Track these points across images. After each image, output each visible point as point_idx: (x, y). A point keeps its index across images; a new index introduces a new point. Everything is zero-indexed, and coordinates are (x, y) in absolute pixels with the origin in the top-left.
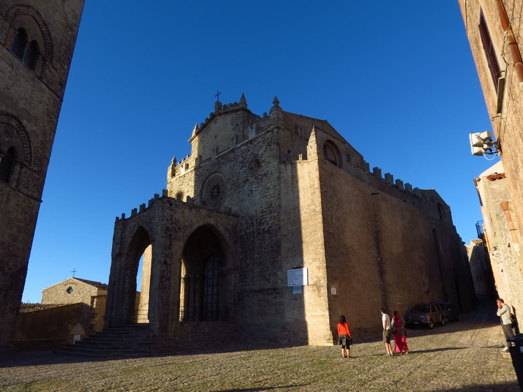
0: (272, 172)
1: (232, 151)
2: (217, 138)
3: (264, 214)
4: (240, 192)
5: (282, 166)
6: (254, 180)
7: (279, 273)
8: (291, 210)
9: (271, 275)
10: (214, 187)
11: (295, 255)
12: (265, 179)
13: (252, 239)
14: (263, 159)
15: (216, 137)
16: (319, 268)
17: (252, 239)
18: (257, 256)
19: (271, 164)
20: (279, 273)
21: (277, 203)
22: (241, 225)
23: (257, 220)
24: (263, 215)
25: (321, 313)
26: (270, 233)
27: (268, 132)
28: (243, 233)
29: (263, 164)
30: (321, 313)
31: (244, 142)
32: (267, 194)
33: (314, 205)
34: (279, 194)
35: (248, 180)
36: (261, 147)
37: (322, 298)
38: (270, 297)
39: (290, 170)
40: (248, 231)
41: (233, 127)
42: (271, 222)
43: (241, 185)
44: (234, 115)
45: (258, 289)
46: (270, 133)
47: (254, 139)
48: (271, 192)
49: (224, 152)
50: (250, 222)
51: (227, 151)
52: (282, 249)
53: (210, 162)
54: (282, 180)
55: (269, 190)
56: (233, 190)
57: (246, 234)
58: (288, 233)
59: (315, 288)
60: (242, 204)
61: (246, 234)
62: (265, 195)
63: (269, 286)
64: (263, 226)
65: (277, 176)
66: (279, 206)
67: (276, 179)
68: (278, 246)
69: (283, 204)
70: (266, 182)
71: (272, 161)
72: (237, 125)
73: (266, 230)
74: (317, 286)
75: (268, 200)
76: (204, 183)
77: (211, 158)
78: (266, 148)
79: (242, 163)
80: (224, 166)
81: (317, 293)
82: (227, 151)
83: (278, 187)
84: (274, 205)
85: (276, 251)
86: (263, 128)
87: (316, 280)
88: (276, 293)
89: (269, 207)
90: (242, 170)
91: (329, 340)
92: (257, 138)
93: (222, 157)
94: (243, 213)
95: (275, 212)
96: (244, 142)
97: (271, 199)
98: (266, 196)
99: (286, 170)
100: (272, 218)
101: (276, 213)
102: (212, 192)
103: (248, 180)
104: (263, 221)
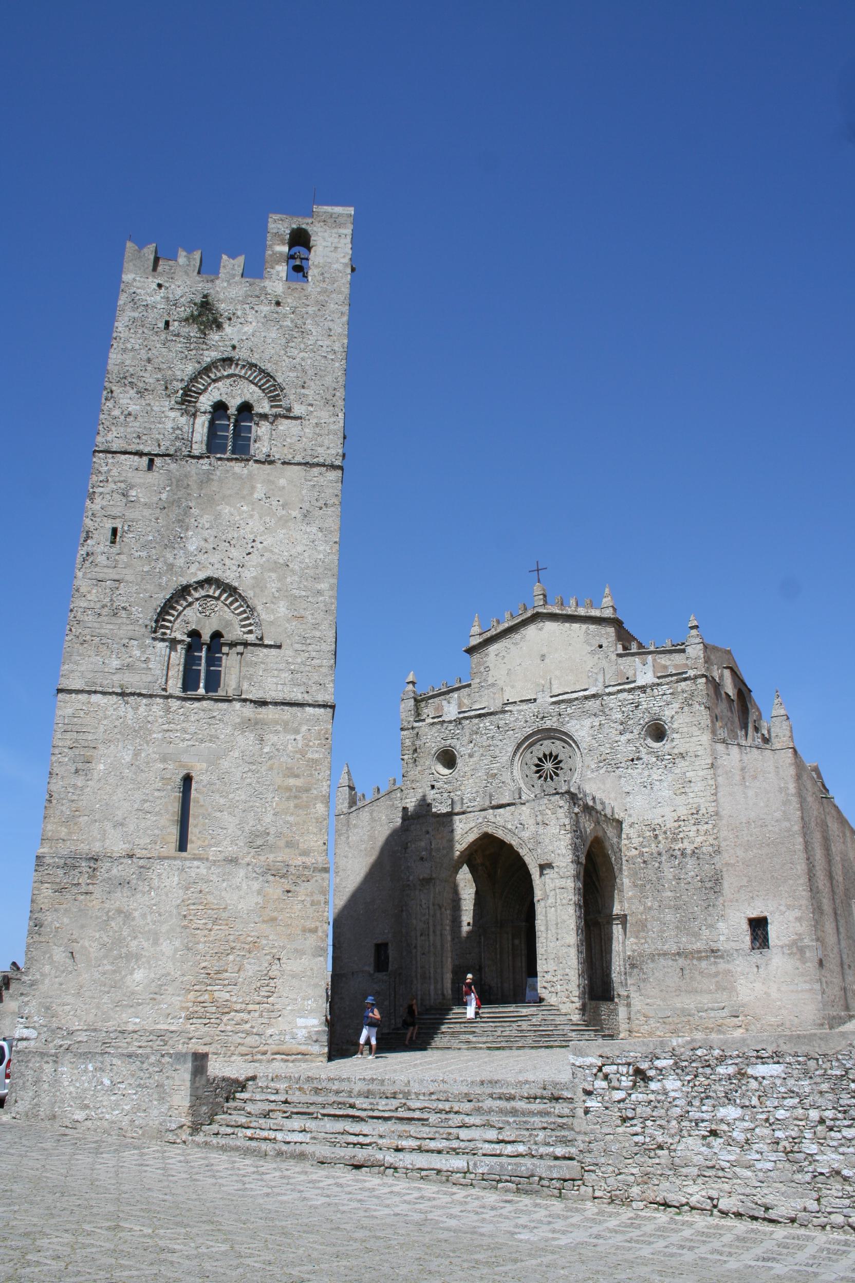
0: (699, 753)
1: (594, 696)
2: (547, 661)
3: (682, 823)
4: (620, 777)
5: (720, 747)
6: (654, 759)
7: (721, 925)
8: (741, 823)
9: (704, 928)
10: (545, 756)
11: (752, 897)
12: (681, 763)
13: (657, 865)
14: (674, 726)
15: (543, 658)
16: (798, 919)
17: (657, 865)
18: (669, 894)
20: (721, 925)
21: (711, 809)
22: (629, 838)
23: (665, 833)
24: (679, 827)
25: (808, 986)
26: (698, 858)
27: (685, 679)
28: (635, 852)
29: (675, 736)
30: (808, 986)
31: (627, 687)
32: (687, 790)
33: (789, 820)
34: (715, 794)
35: (639, 759)
37: (808, 964)
38: (704, 964)
40: (645, 850)
41: (589, 649)
42: (699, 839)
44: (592, 627)
45: (674, 950)
46: (688, 682)
47: (653, 686)
48: (696, 789)
50: (648, 834)
51: (582, 694)
52: (726, 885)
54: (720, 771)
55: (692, 784)
56: (602, 771)
57: (642, 854)
58: (738, 862)
59: (795, 950)
60: (628, 800)
61: (642, 854)
63: (699, 945)
64: (680, 845)
65: (710, 762)
66: (717, 814)
68: (717, 880)
69: (723, 813)
70: (686, 769)
71: (695, 734)
72: (601, 646)
73: (689, 852)
74: (797, 947)
75: (691, 801)
76: (519, 746)
77: (535, 700)
78: (682, 708)
80: (573, 722)
81: (798, 956)
82: (582, 694)
83: (712, 782)
85: (711, 888)
86: (665, 667)
87: (796, 937)
88: (716, 957)
89: (692, 814)
90: (623, 738)
91: (822, 1025)
92: (658, 685)
93: (570, 701)
94: (630, 816)
95: (707, 823)
96: (627, 687)
97: (696, 800)
100: (703, 833)
101: (710, 826)
102: (537, 765)
104: (681, 835)
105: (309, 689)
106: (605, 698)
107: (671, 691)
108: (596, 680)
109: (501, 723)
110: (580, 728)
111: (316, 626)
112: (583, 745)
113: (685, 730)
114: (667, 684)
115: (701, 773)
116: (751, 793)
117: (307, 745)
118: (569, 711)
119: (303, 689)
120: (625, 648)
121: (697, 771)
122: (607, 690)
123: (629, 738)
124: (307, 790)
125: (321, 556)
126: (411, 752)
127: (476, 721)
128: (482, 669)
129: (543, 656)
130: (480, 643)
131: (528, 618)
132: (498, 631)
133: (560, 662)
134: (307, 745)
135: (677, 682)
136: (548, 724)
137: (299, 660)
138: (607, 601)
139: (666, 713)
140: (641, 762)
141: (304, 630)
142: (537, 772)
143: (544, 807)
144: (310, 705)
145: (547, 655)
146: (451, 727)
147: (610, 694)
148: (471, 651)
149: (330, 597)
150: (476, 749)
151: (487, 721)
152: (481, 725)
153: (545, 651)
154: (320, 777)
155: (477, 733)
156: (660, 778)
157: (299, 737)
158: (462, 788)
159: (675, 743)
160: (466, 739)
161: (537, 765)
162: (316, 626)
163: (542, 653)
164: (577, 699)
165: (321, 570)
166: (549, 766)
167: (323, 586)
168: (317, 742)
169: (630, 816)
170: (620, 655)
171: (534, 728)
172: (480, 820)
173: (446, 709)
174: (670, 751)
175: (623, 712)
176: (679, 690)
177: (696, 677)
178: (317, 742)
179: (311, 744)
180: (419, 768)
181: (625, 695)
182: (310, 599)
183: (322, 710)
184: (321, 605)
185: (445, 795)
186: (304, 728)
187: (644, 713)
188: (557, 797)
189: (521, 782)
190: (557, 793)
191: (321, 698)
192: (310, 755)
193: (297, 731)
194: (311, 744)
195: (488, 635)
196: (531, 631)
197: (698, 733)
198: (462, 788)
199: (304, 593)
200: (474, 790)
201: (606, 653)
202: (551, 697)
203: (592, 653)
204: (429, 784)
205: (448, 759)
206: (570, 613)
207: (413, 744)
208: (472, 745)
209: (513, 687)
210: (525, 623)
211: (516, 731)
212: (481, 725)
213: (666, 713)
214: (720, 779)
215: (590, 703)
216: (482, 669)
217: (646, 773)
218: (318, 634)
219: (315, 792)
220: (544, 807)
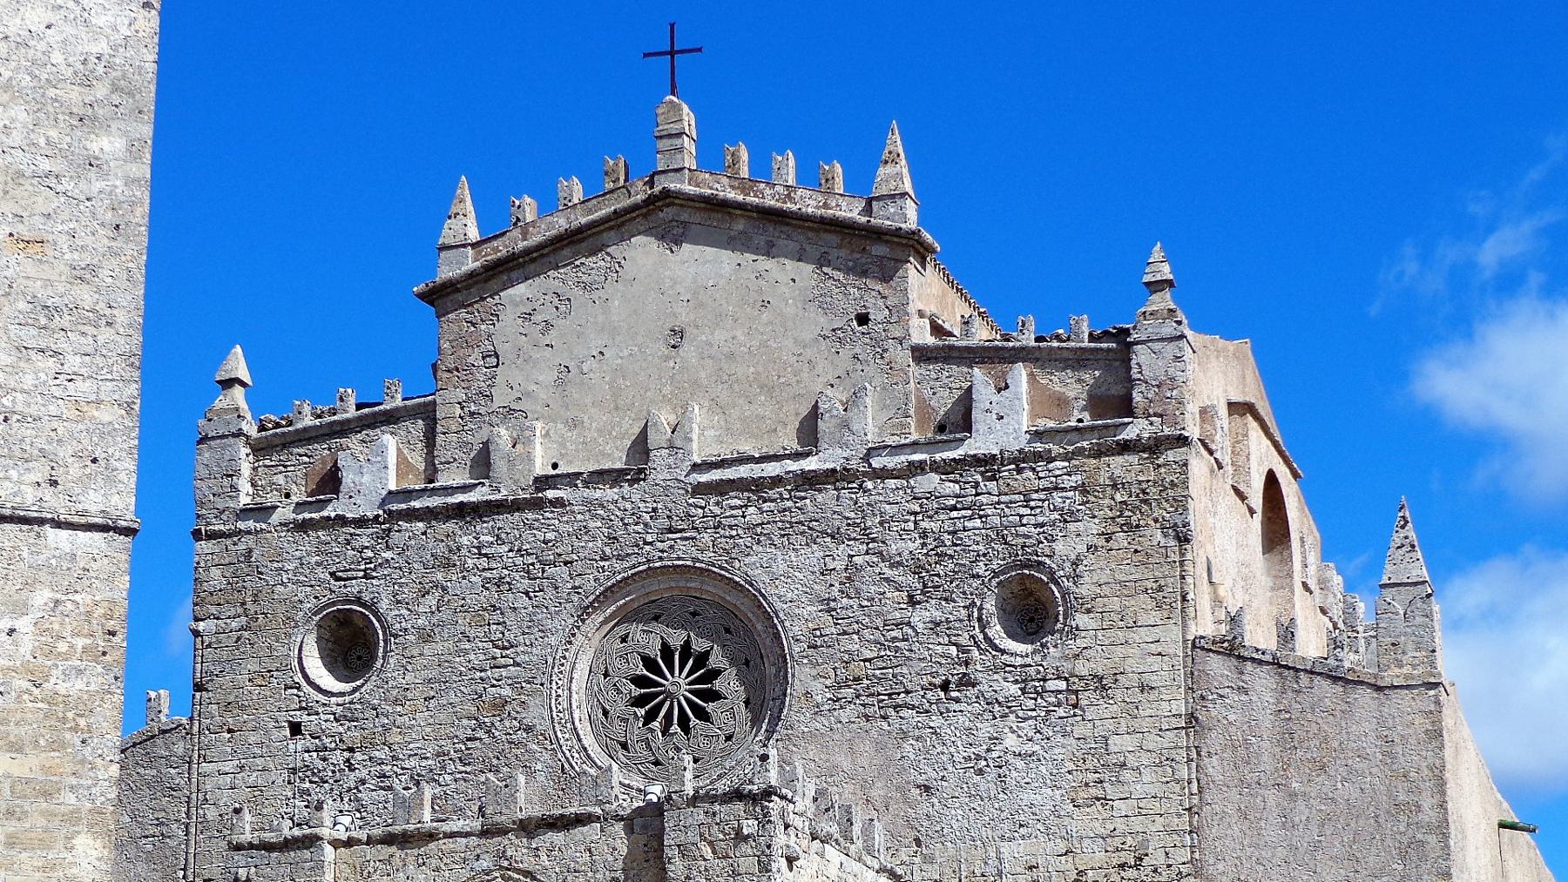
0: (1154, 680)
2: (687, 349)
4: (904, 735)
5: (1217, 666)
6: (1014, 689)
19: (1143, 634)
27: (1125, 447)
29: (1081, 620)
32: (1110, 791)
35: (966, 682)
36: (1068, 517)
39: (1269, 697)
41: (825, 322)
43: (913, 699)
46: (1133, 459)
47: (1021, 460)
49: (772, 469)
53: (634, 492)
54: (1214, 740)
55: (1127, 775)
56: (846, 715)
62: (1100, 794)
67: (1175, 723)
72: (863, 319)
75: (1120, 825)
79: (917, 570)
84: (1158, 859)
89: (1122, 866)
92: (1038, 456)
93: (756, 486)
98: (1104, 800)
99: (1243, 690)
102: (639, 681)
103: (966, 682)
105: (59, 473)
106: (869, 485)
107: (1077, 479)
108: (846, 425)
110: (789, 578)
111: (83, 274)
112: (797, 629)
113: (1115, 604)
114: (1067, 457)
115: (1152, 742)
116: (1301, 812)
117: (51, 652)
119: (40, 472)
120: (937, 330)
121: (1140, 735)
122: (877, 463)
123: (938, 615)
124: (47, 795)
125: (102, 47)
127: (450, 526)
128: (475, 358)
129: (679, 333)
130: (472, 275)
131: (635, 207)
132: (535, 239)
133: (731, 356)
134: (51, 652)
135: (1098, 453)
136: (684, 552)
137: (29, 381)
138: (897, 174)
139: (1059, 546)
140: (971, 692)
141: (48, 283)
142: (639, 702)
143: (692, 836)
144: (58, 524)
145: (689, 332)
146: (364, 538)
147: (883, 474)
148: (441, 296)
149: (130, 181)
151: (484, 531)
152: (465, 540)
153: (684, 317)
154: (87, 751)
155: (448, 565)
156: (1029, 747)
157: (24, 624)
158: (395, 737)
159: (1081, 643)
161: (639, 681)
162: (83, 274)
164: (777, 481)
165: (101, 91)
166: (679, 683)
167: (108, 144)
168: (80, 642)
169: (928, 859)
170: (922, 355)
171: (637, 563)
172: (485, 864)
173: (348, 478)
174: (1067, 666)
175: (924, 535)
176: (1103, 478)
177: (1154, 447)
178: (80, 642)
179: (62, 647)
181: (930, 481)
182: (67, 185)
183: (97, 536)
184: (101, 207)
185: (338, 757)
186: (42, 597)
187: (988, 540)
188: (739, 807)
189: (584, 729)
190: (737, 795)
191: (94, 503)
192: (58, 684)
193: (21, 609)
194: (62, 647)
195: (502, 248)
196: (642, 252)
197: (1154, 617)
198: (395, 737)
199: (45, 165)
200: (431, 749)
201: (876, 342)
202: (696, 467)
203: (837, 336)
205: (352, 642)
206: (770, 202)
208: (432, 600)
209: (574, 424)
210: (620, 224)
211: (578, 566)
212: (465, 540)
213: (1059, 546)
214: (1213, 766)
215: (820, 498)
216: (475, 358)
217: (985, 729)
218: (86, 296)
219: (71, 799)
220: (692, 836)
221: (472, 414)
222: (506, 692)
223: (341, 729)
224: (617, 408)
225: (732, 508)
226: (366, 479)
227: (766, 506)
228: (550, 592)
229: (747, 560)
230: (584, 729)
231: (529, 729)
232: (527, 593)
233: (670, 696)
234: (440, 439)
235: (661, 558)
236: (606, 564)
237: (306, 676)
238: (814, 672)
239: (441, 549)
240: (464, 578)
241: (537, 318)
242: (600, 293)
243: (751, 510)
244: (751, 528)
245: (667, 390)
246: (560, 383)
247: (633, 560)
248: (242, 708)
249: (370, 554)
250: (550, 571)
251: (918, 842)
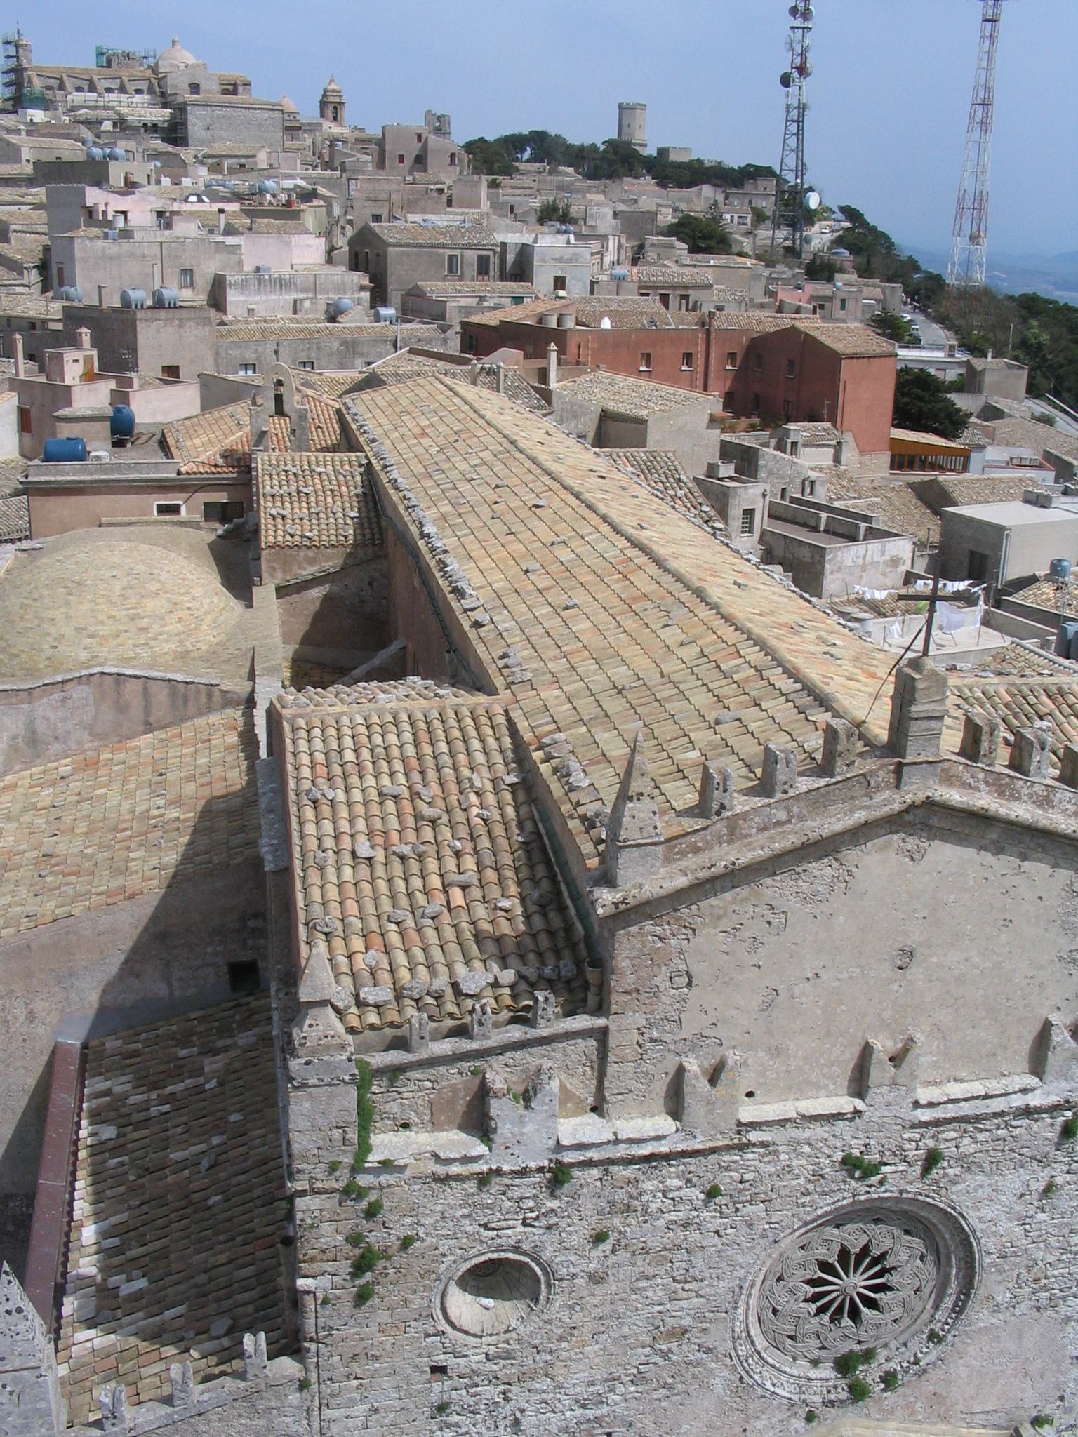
2: (916, 972)
10: (844, 1254)
109: (725, 1181)
118: (967, 1146)
126: (345, 1266)
127: (630, 1172)
133: (960, 980)
146: (524, 1187)
150: (622, 1256)
153: (915, 936)
155: (628, 1210)
160: (578, 1234)
163: (908, 942)
180: (383, 1316)
189: (755, 1330)
196: (878, 863)
200: (600, 1375)
204: (425, 1363)
207: (354, 1239)
208: (607, 1246)
209: (776, 1051)
212: (649, 1185)
215: (1035, 1127)
221: (652, 1040)
222: (686, 1322)
223: (495, 1368)
224: (828, 1034)
225: (947, 1140)
226: (528, 1129)
227: (980, 1137)
228: (744, 1230)
229: (954, 1189)
230: (755, 1330)
231: (709, 1351)
232: (717, 1232)
233: (844, 1292)
234: (611, 1069)
235: (868, 1192)
236: (808, 1199)
237: (444, 1309)
238: (1000, 1278)
239: (620, 1196)
240: (645, 1222)
241: (746, 934)
242: (824, 907)
243: (967, 1141)
244: (961, 1159)
245: (887, 1014)
246: (767, 1007)
247: (840, 1196)
248: (375, 1358)
249: (531, 1204)
250: (748, 1209)
251: (1062, 1398)
